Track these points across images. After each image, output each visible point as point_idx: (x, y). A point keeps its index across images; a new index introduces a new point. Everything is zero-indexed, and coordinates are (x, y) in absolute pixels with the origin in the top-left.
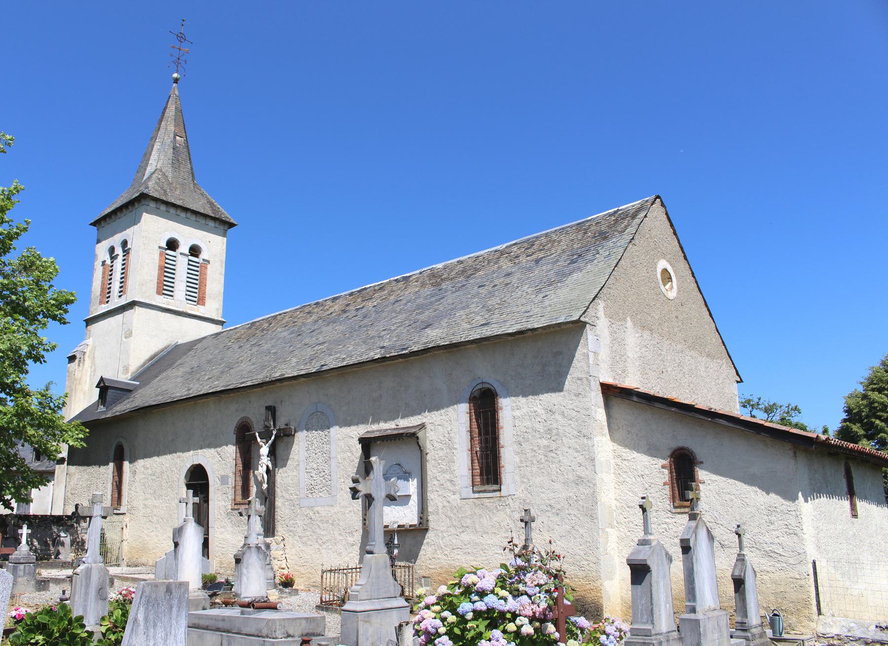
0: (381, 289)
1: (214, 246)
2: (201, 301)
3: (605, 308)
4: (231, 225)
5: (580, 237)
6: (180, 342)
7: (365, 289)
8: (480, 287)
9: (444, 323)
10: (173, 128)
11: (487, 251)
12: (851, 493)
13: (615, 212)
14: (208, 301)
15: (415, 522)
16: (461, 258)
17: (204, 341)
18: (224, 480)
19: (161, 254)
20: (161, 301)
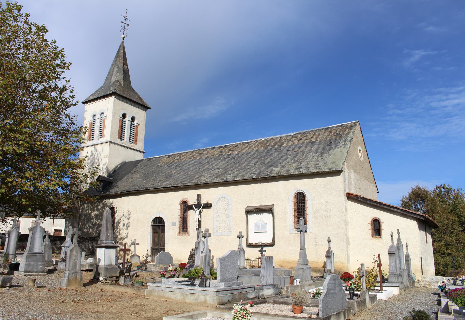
0: (236, 146)
1: (140, 116)
2: (136, 143)
3: (347, 165)
4: (149, 108)
5: (328, 134)
6: (127, 161)
7: (227, 145)
8: (288, 151)
9: (279, 165)
10: (123, 61)
11: (285, 135)
12: (426, 231)
13: (341, 126)
14: (138, 142)
15: (271, 241)
16: (274, 137)
17: (142, 162)
18: (174, 224)
19: (120, 120)
20: (118, 141)
